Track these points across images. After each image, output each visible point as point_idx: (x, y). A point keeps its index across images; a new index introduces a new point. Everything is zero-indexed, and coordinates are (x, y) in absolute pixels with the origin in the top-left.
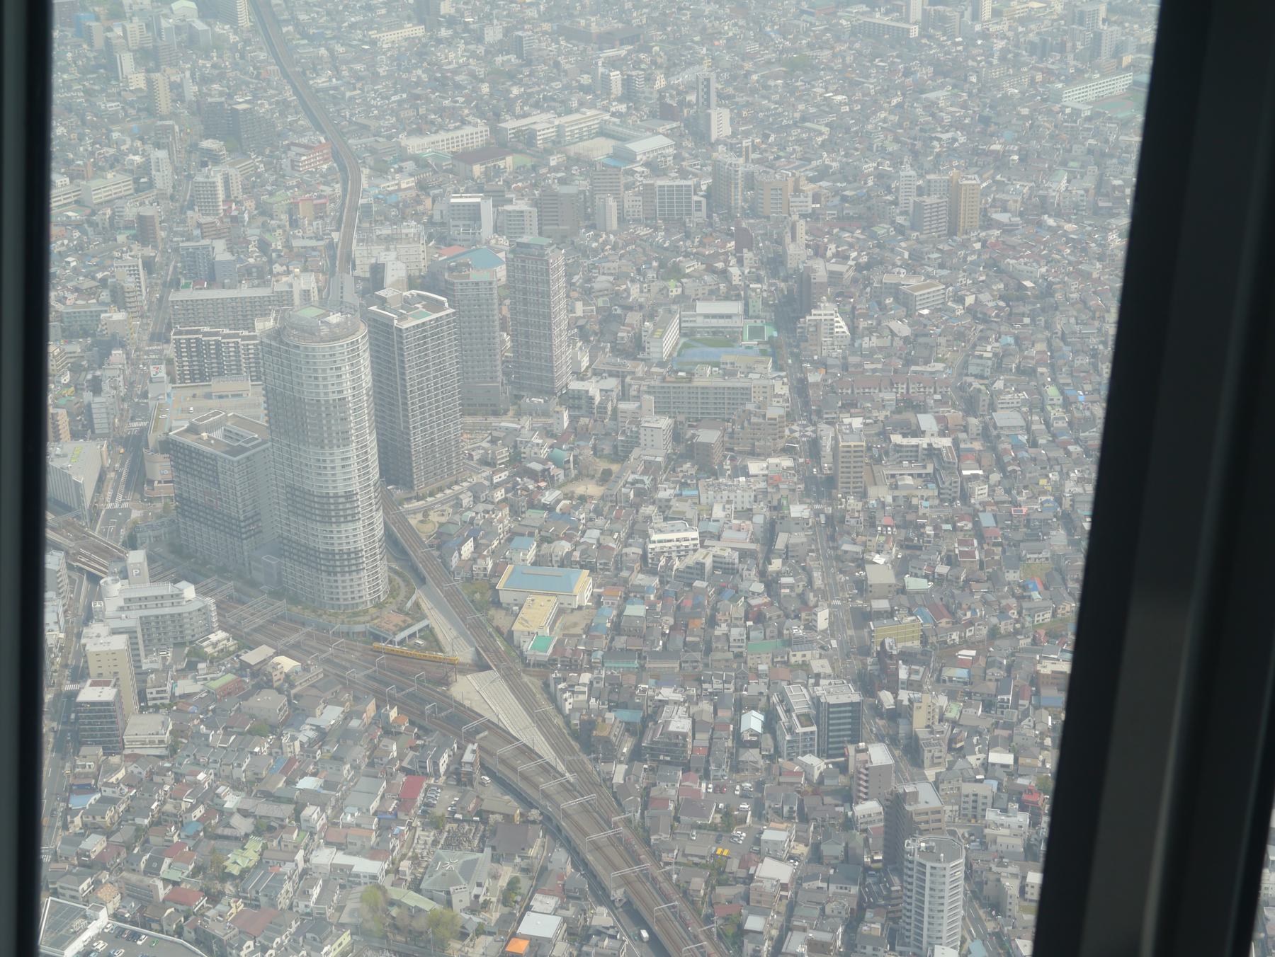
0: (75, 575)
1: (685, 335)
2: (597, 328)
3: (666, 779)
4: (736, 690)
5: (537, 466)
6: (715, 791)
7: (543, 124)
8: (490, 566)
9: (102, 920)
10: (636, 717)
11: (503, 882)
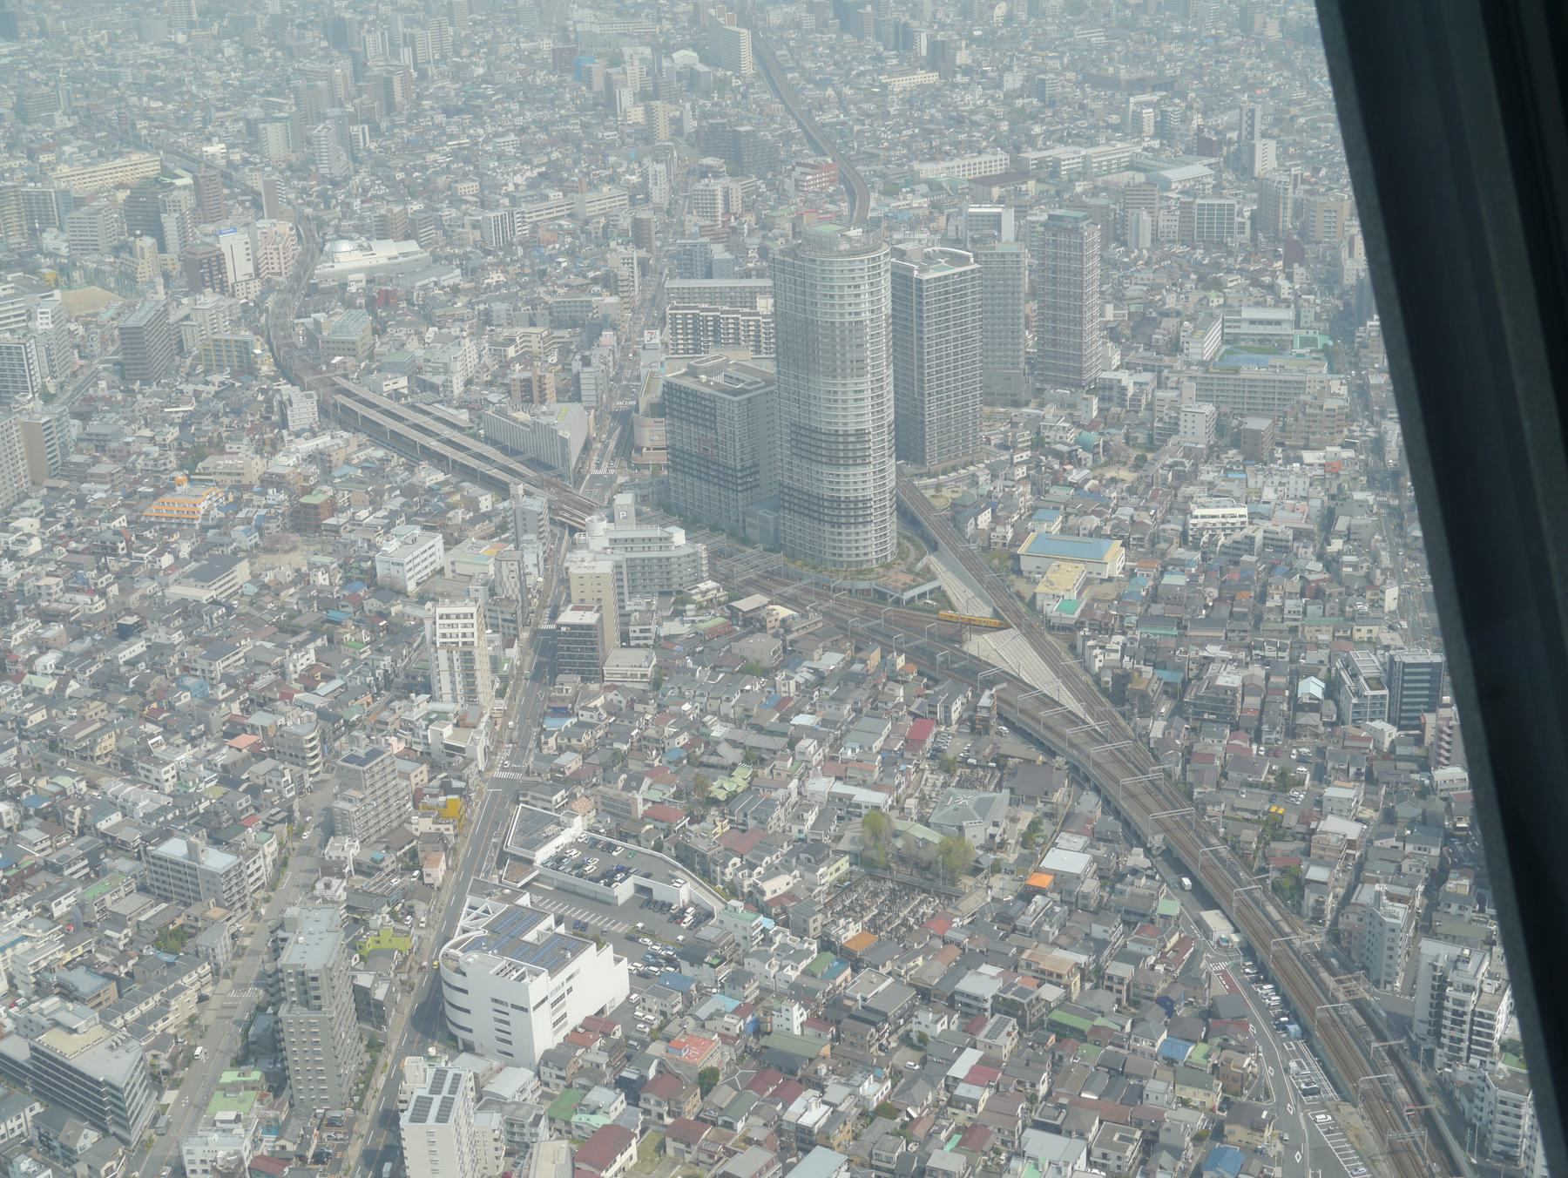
0: (557, 530)
1: (1228, 342)
2: (1128, 332)
4: (1292, 661)
5: (1065, 449)
6: (1267, 754)
8: (1010, 535)
9: (576, 829)
10: (1177, 678)
11: (1023, 826)
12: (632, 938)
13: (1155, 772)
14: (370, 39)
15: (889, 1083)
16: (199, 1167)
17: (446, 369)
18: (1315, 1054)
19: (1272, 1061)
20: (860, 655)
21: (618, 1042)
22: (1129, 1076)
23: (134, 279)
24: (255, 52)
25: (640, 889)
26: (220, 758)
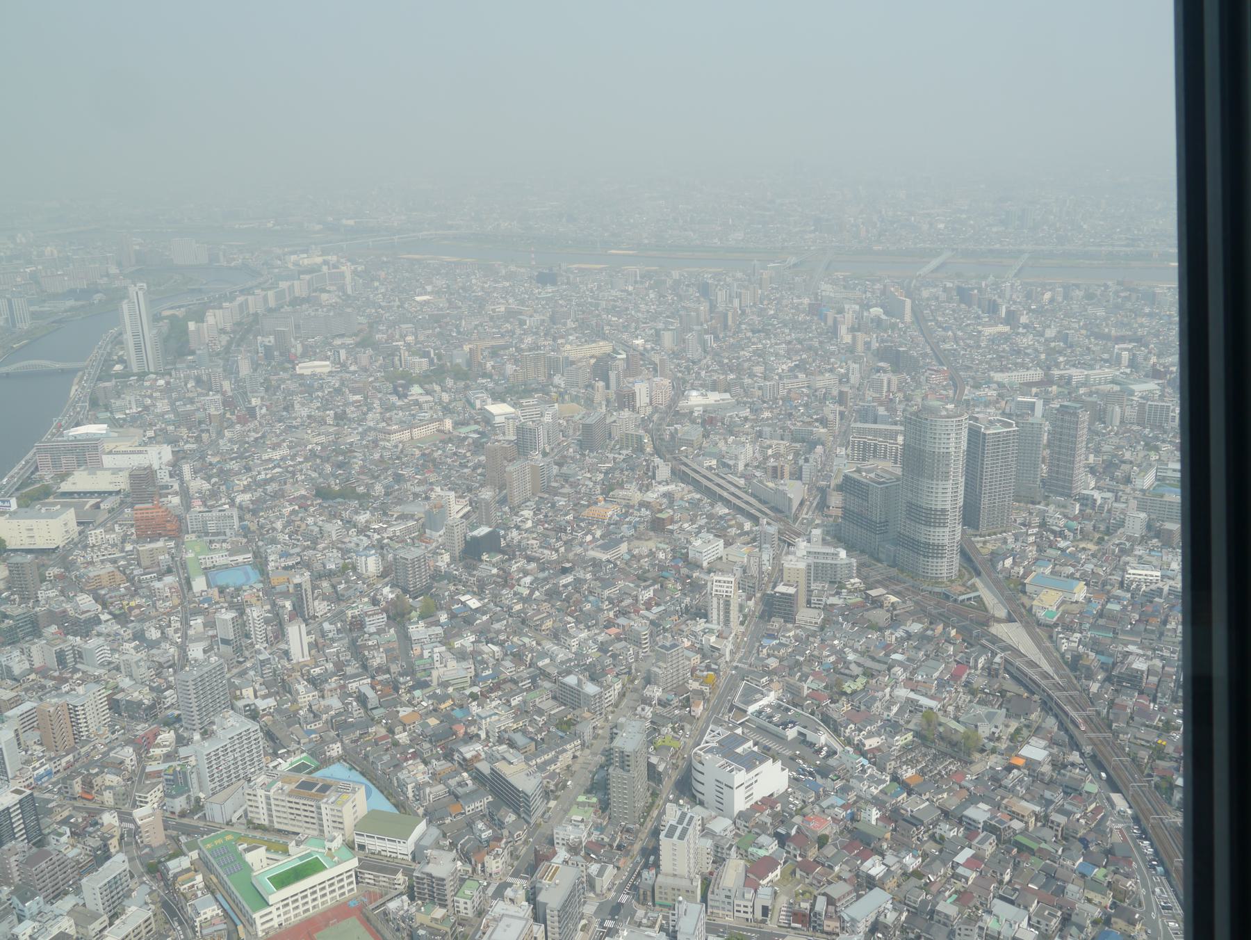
0: (782, 545)
1: (1159, 480)
3: (1127, 695)
5: (1058, 529)
6: (1159, 710)
7: (1077, 374)
8: (1021, 572)
10: (1110, 661)
11: (1012, 730)
12: (793, 759)
13: (1090, 711)
14: (719, 293)
15: (920, 859)
16: (561, 842)
17: (736, 458)
18: (1172, 886)
19: (1145, 885)
20: (933, 626)
21: (778, 813)
22: (1058, 879)
23: (593, 401)
24: (664, 297)
25: (800, 733)
26: (600, 638)
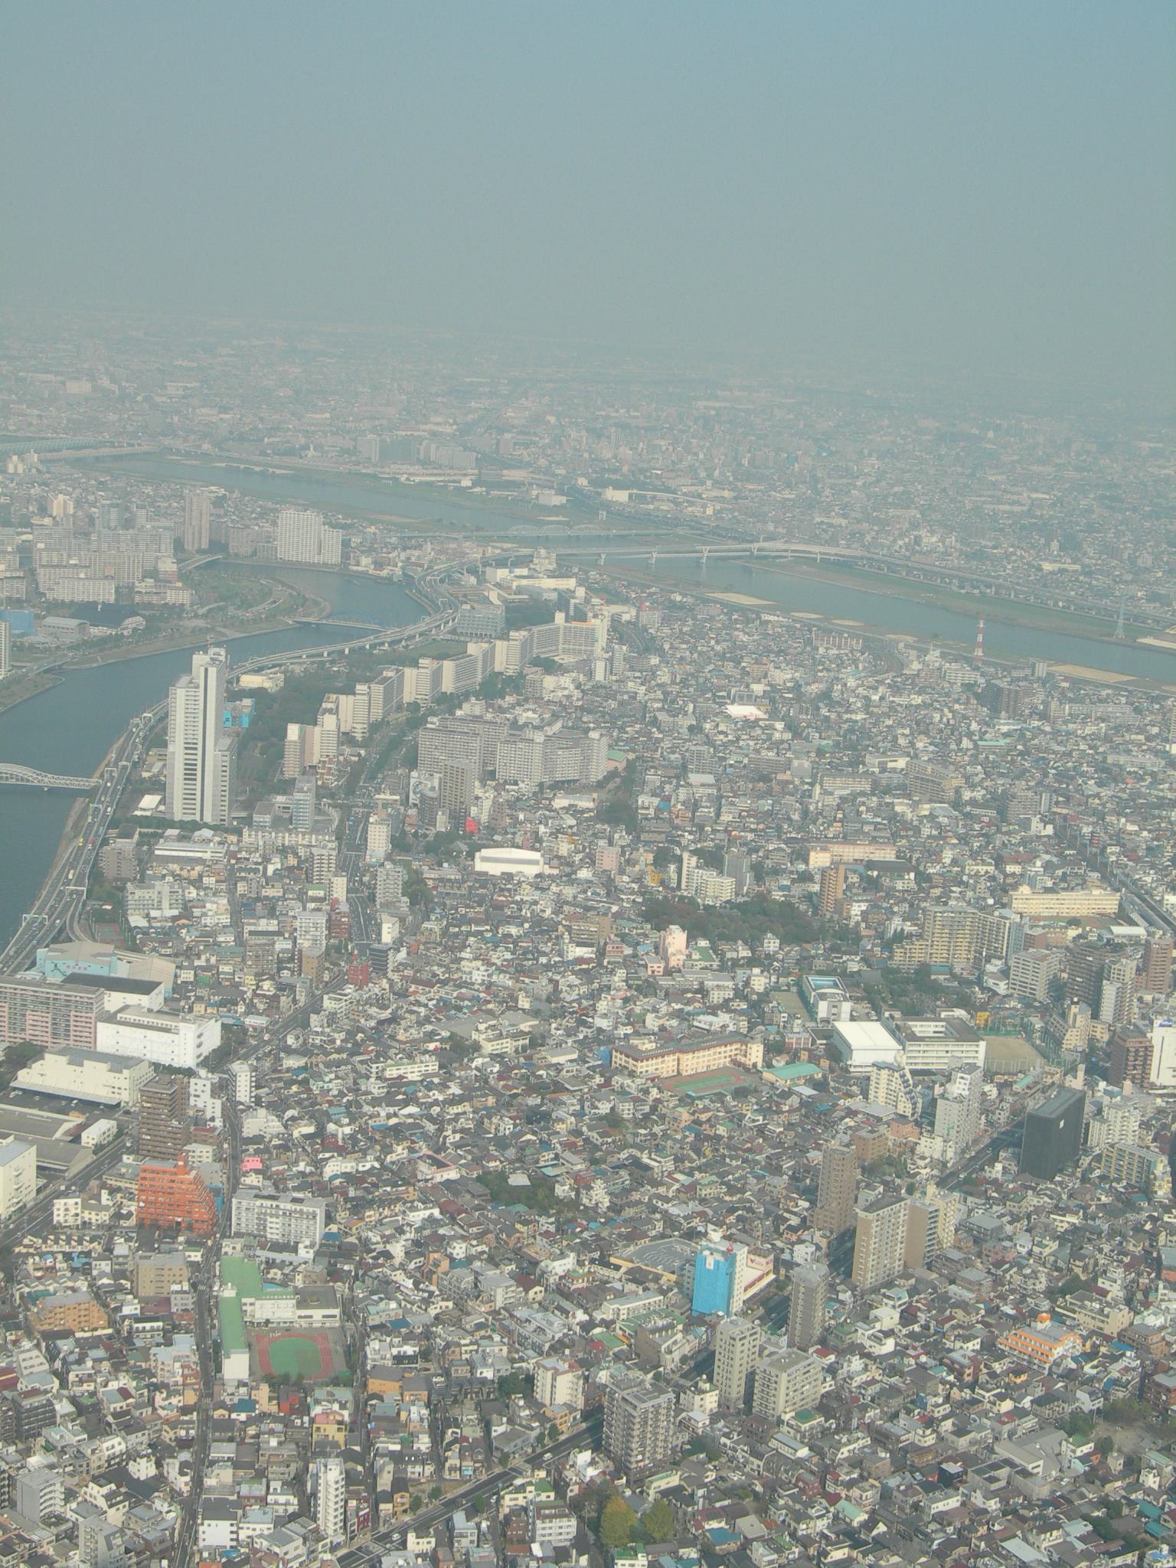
23: (1059, 1043)
